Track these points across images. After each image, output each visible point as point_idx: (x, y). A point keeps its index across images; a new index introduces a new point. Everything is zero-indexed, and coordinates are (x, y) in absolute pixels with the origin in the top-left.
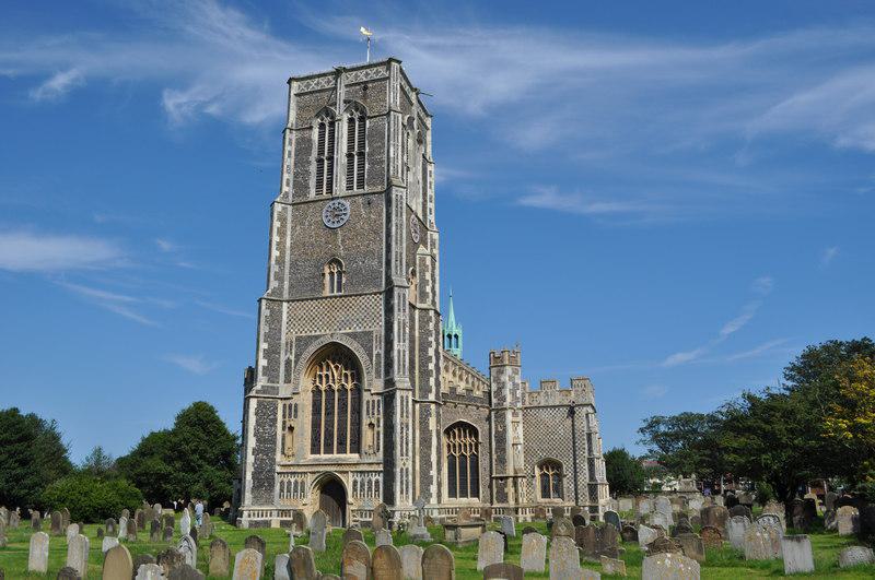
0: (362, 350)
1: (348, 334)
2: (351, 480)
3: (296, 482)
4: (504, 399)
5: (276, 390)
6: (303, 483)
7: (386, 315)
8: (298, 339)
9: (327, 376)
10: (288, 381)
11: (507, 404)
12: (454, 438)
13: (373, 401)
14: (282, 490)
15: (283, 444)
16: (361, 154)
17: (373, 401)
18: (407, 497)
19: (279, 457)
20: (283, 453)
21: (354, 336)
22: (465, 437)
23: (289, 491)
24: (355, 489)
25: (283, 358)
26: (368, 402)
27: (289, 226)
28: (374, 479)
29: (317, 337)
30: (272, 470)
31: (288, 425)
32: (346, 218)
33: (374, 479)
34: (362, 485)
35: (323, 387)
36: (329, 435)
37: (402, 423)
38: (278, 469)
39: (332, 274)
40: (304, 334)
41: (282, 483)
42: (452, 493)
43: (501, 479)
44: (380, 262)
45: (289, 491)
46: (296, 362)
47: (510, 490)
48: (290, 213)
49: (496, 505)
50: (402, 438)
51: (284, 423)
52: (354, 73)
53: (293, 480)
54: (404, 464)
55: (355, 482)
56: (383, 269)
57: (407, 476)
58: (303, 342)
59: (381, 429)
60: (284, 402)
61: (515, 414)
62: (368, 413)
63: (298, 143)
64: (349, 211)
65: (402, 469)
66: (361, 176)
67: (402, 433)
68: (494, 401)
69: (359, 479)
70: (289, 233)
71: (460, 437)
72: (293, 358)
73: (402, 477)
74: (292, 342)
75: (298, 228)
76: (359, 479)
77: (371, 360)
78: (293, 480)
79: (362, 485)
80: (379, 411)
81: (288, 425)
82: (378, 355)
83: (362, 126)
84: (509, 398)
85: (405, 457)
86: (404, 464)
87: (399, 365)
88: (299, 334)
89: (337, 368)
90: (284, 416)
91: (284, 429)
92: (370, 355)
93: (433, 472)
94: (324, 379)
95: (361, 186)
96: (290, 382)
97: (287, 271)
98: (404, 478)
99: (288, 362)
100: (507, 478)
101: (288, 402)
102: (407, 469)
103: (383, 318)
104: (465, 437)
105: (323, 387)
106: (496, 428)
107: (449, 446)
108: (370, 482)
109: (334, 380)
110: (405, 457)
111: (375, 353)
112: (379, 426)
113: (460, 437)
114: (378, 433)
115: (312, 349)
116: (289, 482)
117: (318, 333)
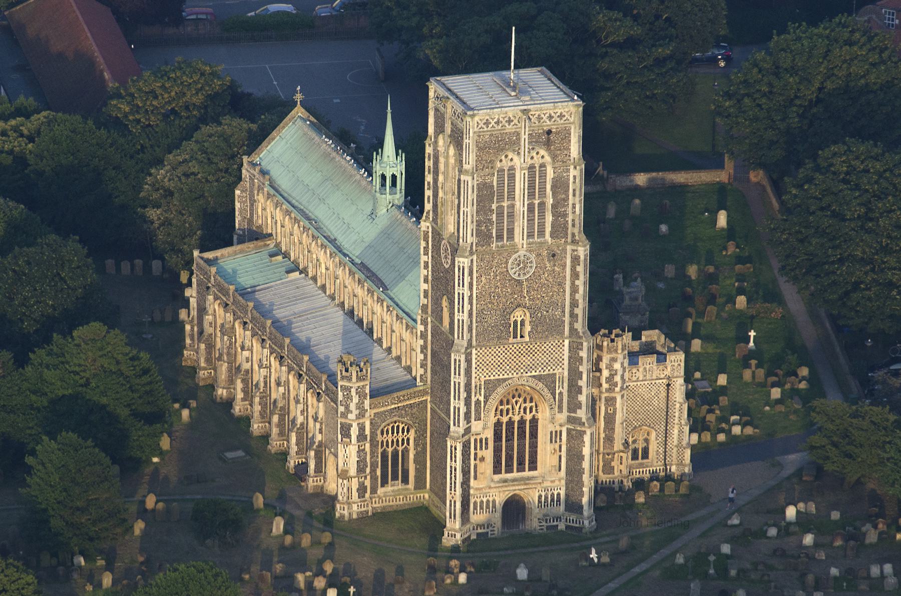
1: (534, 376)
2: (537, 495)
7: (569, 360)
15: (475, 472)
17: (556, 432)
20: (475, 478)
26: (551, 433)
29: (505, 380)
36: (509, 458)
40: (492, 378)
44: (563, 312)
46: (485, 402)
51: (476, 454)
56: (567, 319)
59: (564, 454)
69: (543, 494)
72: (482, 399)
75: (483, 279)
76: (543, 494)
77: (555, 398)
80: (560, 439)
88: (487, 378)
90: (476, 449)
91: (475, 459)
96: (480, 419)
99: (478, 402)
103: (566, 362)
111: (557, 392)
112: (560, 451)
114: (560, 457)
115: (500, 391)
117: (506, 376)
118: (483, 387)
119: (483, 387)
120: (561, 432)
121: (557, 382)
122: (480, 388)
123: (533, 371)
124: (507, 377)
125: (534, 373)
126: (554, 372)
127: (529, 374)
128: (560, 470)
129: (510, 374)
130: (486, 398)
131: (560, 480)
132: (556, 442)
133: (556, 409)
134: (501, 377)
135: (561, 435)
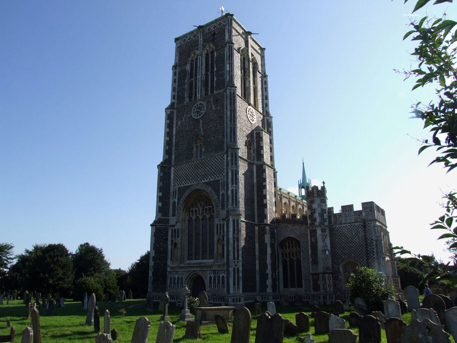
0: (213, 192)
3: (178, 277)
4: (315, 220)
5: (168, 221)
6: (182, 278)
8: (180, 189)
9: (196, 211)
10: (174, 215)
11: (317, 223)
12: (286, 248)
13: (220, 225)
14: (171, 283)
16: (212, 72)
17: (220, 225)
18: (238, 288)
19: (169, 262)
20: (171, 260)
21: (209, 184)
22: (292, 247)
23: (174, 283)
24: (210, 283)
25: (172, 201)
27: (175, 121)
28: (221, 276)
30: (165, 271)
31: (174, 242)
32: (204, 112)
33: (221, 276)
34: (215, 280)
35: (194, 218)
37: (234, 238)
38: (169, 269)
39: (197, 147)
40: (182, 186)
41: (171, 278)
42: (286, 286)
43: (316, 274)
45: (174, 283)
46: (178, 203)
47: (320, 282)
48: (175, 115)
49: (313, 293)
50: (234, 247)
51: (172, 240)
52: (208, 27)
53: (176, 276)
54: (236, 265)
55: (210, 278)
57: (238, 273)
58: (182, 190)
60: (172, 228)
61: (323, 231)
62: (217, 233)
63: (179, 74)
64: (205, 108)
65: (234, 269)
66: (212, 86)
67: (234, 244)
68: (309, 222)
69: (213, 276)
70: (175, 126)
71: (289, 248)
72: (176, 201)
73: (234, 273)
74: (176, 191)
76: (213, 276)
77: (219, 198)
78: (176, 276)
79: (215, 280)
80: (224, 231)
81: (174, 242)
82: (223, 194)
83: (213, 56)
84: (318, 220)
85: (236, 261)
86: (236, 265)
87: (233, 200)
89: (201, 205)
91: (172, 245)
92: (218, 195)
93: (269, 271)
94: (194, 213)
95: (212, 91)
97: (174, 148)
98: (236, 275)
99: (174, 203)
100: (319, 274)
101: (174, 228)
102: (238, 269)
104: (292, 247)
105: (194, 218)
106: (311, 240)
107: (283, 254)
108: (219, 277)
109: (199, 213)
110: (236, 261)
111: (221, 193)
113: (289, 248)
116: (175, 278)
117: (190, 184)
118: (177, 192)
119: (177, 192)
120: (224, 224)
121: (221, 186)
122: (176, 194)
123: (206, 179)
124: (190, 184)
125: (206, 181)
126: (219, 179)
127: (203, 181)
128: (223, 256)
129: (192, 182)
130: (179, 200)
131: (224, 265)
132: (220, 233)
133: (220, 207)
134: (187, 185)
135: (224, 228)
